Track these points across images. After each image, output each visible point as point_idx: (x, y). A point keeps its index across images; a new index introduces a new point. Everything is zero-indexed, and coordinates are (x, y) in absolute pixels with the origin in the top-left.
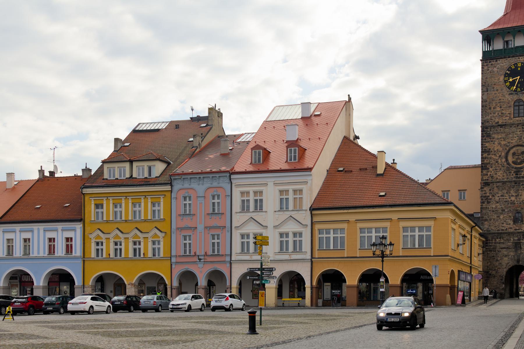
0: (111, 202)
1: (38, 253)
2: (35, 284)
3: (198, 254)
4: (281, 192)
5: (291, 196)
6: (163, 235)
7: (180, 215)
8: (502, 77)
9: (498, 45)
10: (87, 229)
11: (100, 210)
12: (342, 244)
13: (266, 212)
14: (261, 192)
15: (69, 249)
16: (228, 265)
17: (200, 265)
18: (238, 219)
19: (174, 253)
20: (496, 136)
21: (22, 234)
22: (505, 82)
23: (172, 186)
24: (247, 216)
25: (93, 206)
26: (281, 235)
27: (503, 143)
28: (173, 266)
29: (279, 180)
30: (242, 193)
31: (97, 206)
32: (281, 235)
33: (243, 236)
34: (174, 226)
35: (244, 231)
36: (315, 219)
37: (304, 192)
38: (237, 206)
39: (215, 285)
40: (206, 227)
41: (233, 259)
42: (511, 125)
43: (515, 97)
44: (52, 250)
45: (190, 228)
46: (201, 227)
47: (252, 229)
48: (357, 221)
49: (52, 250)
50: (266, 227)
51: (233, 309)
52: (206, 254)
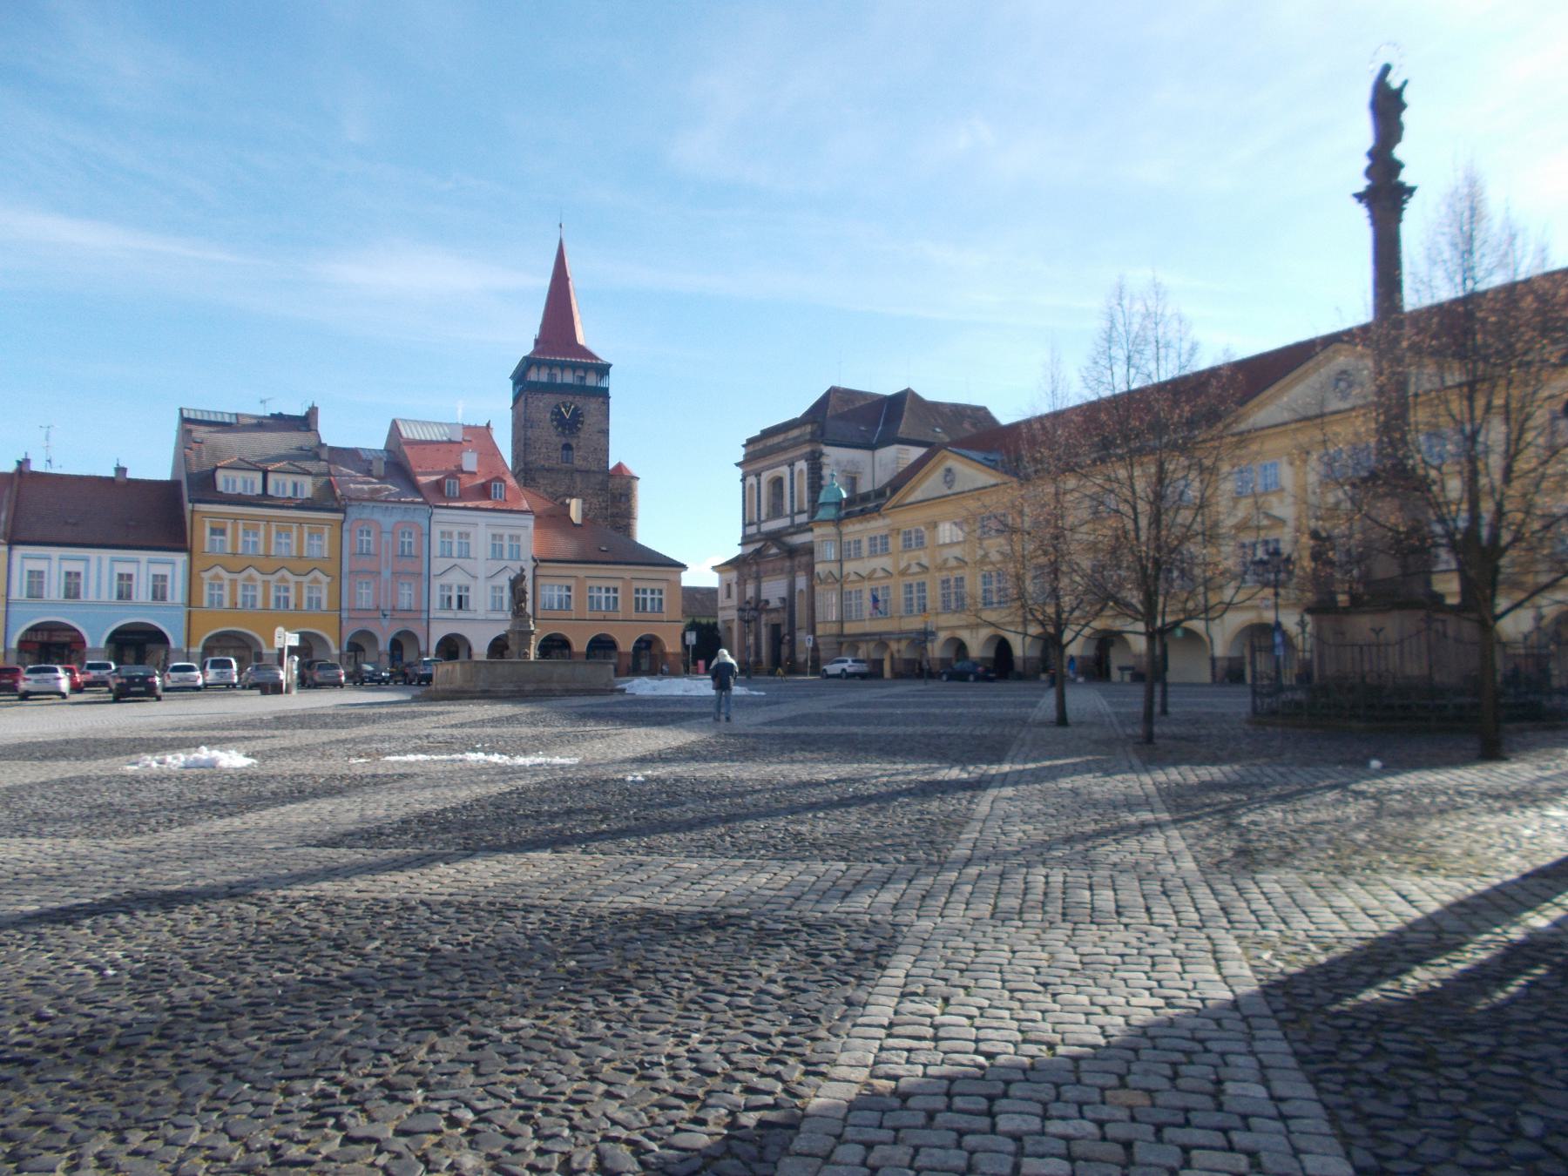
0: (241, 527)
1: (98, 595)
2: (89, 644)
3: (382, 607)
4: (494, 536)
5: (506, 543)
6: (328, 579)
7: (354, 554)
8: (548, 415)
9: (543, 376)
10: (197, 565)
11: (218, 538)
12: (568, 604)
13: (475, 559)
14: (468, 535)
15: (159, 594)
16: (425, 624)
17: (385, 623)
18: (438, 565)
19: (345, 605)
20: (541, 481)
21: (152, 566)
22: (552, 420)
23: (344, 512)
24: (452, 562)
25: (207, 531)
26: (494, 588)
27: (550, 490)
28: (344, 624)
29: (494, 521)
30: (443, 534)
31: (214, 531)
32: (494, 588)
33: (442, 587)
34: (346, 568)
35: (445, 580)
36: (538, 572)
37: (522, 539)
38: (436, 549)
39: (363, 650)
40: (393, 573)
41: (432, 616)
42: (558, 471)
43: (564, 441)
44: (124, 594)
45: (371, 573)
46: (386, 574)
47: (456, 578)
49: (124, 594)
50: (475, 577)
51: (166, 689)
52: (394, 609)
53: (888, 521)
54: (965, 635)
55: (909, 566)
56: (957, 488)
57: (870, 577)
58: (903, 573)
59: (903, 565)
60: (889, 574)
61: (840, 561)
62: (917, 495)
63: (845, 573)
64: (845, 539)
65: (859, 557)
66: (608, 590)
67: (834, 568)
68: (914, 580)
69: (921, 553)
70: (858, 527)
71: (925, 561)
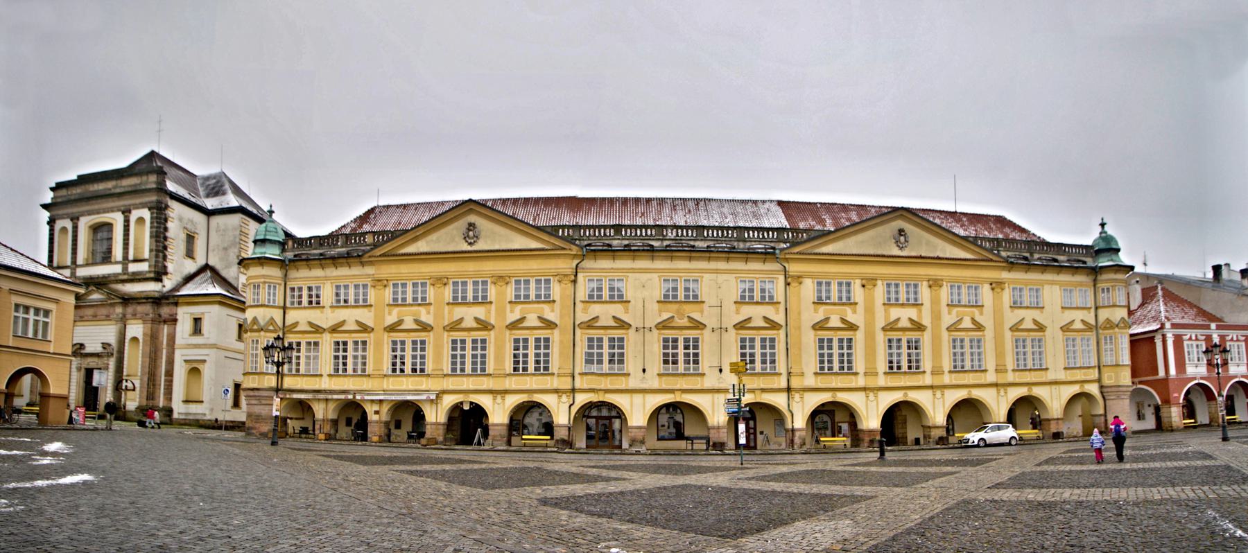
48: (12, 291)
53: (369, 270)
54: (485, 401)
55: (400, 322)
56: (480, 246)
57: (334, 330)
58: (392, 329)
59: (391, 319)
60: (364, 328)
61: (284, 308)
62: (411, 249)
63: (288, 322)
64: (290, 285)
65: (315, 302)
66: (37, 311)
67: (277, 315)
68: (606, 336)
69: (422, 310)
70: (318, 272)
71: (426, 317)
